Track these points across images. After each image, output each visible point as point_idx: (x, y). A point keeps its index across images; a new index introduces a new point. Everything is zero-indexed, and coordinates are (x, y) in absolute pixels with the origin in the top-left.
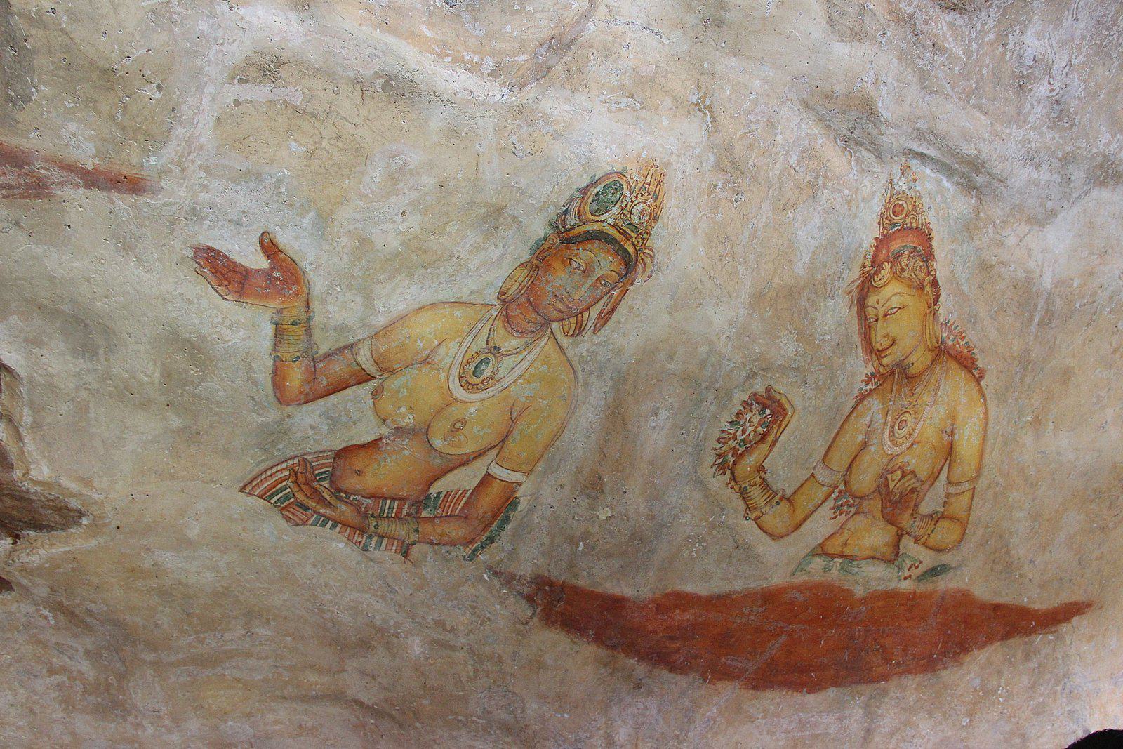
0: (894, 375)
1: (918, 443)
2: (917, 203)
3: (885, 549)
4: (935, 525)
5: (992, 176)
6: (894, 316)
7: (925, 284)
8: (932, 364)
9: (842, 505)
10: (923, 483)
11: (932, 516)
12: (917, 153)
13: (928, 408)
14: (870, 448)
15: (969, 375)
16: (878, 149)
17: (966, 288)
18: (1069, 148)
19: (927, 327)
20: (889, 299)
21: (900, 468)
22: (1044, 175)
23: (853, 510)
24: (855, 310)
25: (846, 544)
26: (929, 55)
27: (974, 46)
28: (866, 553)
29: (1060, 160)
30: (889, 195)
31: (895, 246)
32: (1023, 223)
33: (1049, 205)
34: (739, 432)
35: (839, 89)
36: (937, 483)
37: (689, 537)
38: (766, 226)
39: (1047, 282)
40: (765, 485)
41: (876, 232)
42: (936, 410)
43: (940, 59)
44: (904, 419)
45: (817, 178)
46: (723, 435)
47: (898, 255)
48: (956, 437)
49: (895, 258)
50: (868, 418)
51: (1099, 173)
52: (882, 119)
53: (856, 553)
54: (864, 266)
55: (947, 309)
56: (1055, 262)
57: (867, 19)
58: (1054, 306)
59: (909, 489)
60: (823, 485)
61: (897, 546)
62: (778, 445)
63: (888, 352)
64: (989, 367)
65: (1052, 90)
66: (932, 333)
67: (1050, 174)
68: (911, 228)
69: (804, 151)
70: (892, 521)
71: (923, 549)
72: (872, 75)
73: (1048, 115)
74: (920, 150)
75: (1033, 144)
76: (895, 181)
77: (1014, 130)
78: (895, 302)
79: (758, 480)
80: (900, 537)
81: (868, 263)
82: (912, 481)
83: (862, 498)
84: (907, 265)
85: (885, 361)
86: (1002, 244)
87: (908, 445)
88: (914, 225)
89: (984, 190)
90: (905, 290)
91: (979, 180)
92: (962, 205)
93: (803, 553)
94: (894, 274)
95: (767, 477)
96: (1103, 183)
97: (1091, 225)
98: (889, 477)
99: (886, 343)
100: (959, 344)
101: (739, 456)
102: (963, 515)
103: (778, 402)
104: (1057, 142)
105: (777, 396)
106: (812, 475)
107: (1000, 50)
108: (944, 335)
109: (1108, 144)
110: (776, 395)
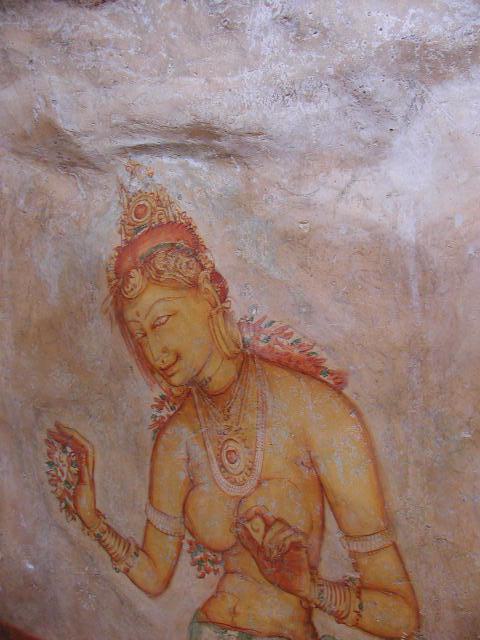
0: (192, 395)
1: (268, 479)
2: (161, 197)
3: (292, 626)
4: (359, 597)
5: (237, 134)
6: (166, 326)
7: (200, 281)
8: (239, 375)
9: (201, 560)
10: (306, 536)
11: (346, 585)
12: (134, 148)
13: (260, 433)
14: (202, 488)
15: (314, 383)
16: (88, 162)
17: (276, 273)
18: (339, 58)
19: (217, 333)
20: (151, 308)
21: (256, 514)
22: (329, 103)
23: (220, 567)
24: (117, 328)
25: (234, 613)
26: (89, 56)
27: (146, 20)
28: (267, 628)
29: (336, 78)
30: (126, 201)
31: (144, 249)
32: (336, 173)
33: (366, 135)
34: (60, 474)
35: (28, 126)
36: (328, 537)
37: (77, 588)
38: (11, 269)
39: (408, 230)
40: (117, 535)
41: (118, 241)
42: (274, 435)
43: (102, 53)
44: (230, 448)
45: (43, 210)
46: (50, 477)
47: (149, 259)
48: (322, 469)
49: (145, 262)
50: (183, 451)
51: (414, 67)
52: (68, 133)
53: (252, 627)
54: (110, 281)
55: (237, 306)
56: (417, 204)
57: (11, 58)
58: (432, 262)
59: (288, 542)
60: (167, 534)
61: (309, 622)
62: (97, 485)
63: (175, 369)
64: (351, 368)
65: (275, 10)
66: (226, 337)
67: (337, 98)
68: (161, 225)
69: (31, 192)
70: (287, 588)
71: (357, 632)
72: (40, 100)
73: (286, 37)
74: (135, 143)
75: (283, 77)
76: (126, 184)
77: (246, 75)
78: (160, 310)
79: (105, 527)
80: (309, 612)
81: (113, 276)
82: (288, 533)
83: (224, 552)
84: (165, 266)
85: (176, 380)
86: (309, 205)
87: (254, 483)
88: (164, 221)
89: (242, 152)
90: (171, 293)
91: (225, 144)
92: (221, 179)
93: (188, 617)
94: (148, 279)
95: (108, 522)
96: (439, 77)
97: (454, 138)
98: (248, 525)
99: (169, 359)
100: (281, 345)
101: (74, 498)
102: (401, 585)
103: (71, 437)
104: (318, 60)
105: (70, 433)
106: (148, 521)
107: (183, 7)
108: (247, 336)
109: (398, 27)
110: (67, 431)
